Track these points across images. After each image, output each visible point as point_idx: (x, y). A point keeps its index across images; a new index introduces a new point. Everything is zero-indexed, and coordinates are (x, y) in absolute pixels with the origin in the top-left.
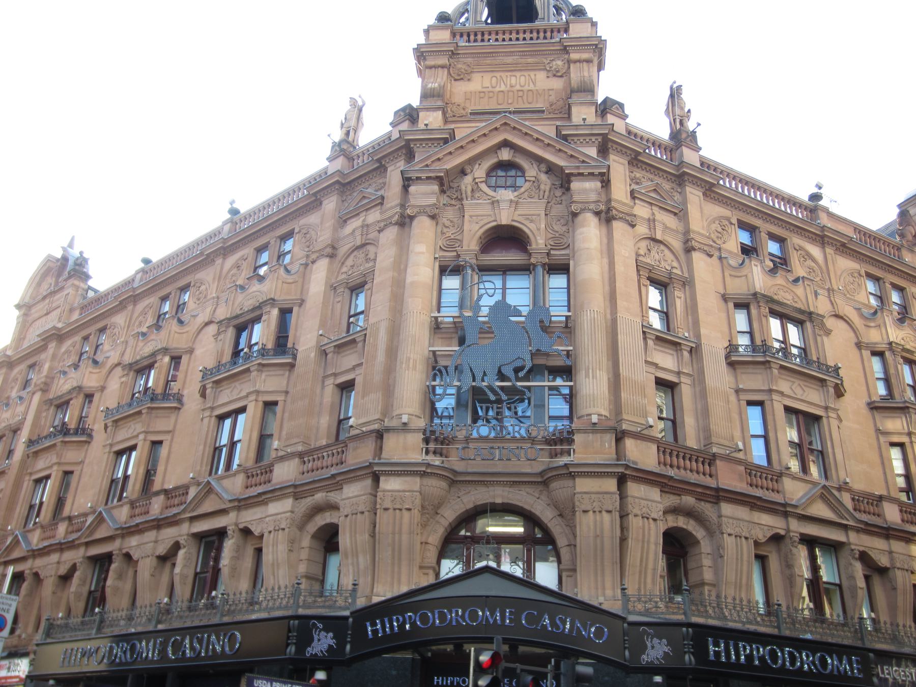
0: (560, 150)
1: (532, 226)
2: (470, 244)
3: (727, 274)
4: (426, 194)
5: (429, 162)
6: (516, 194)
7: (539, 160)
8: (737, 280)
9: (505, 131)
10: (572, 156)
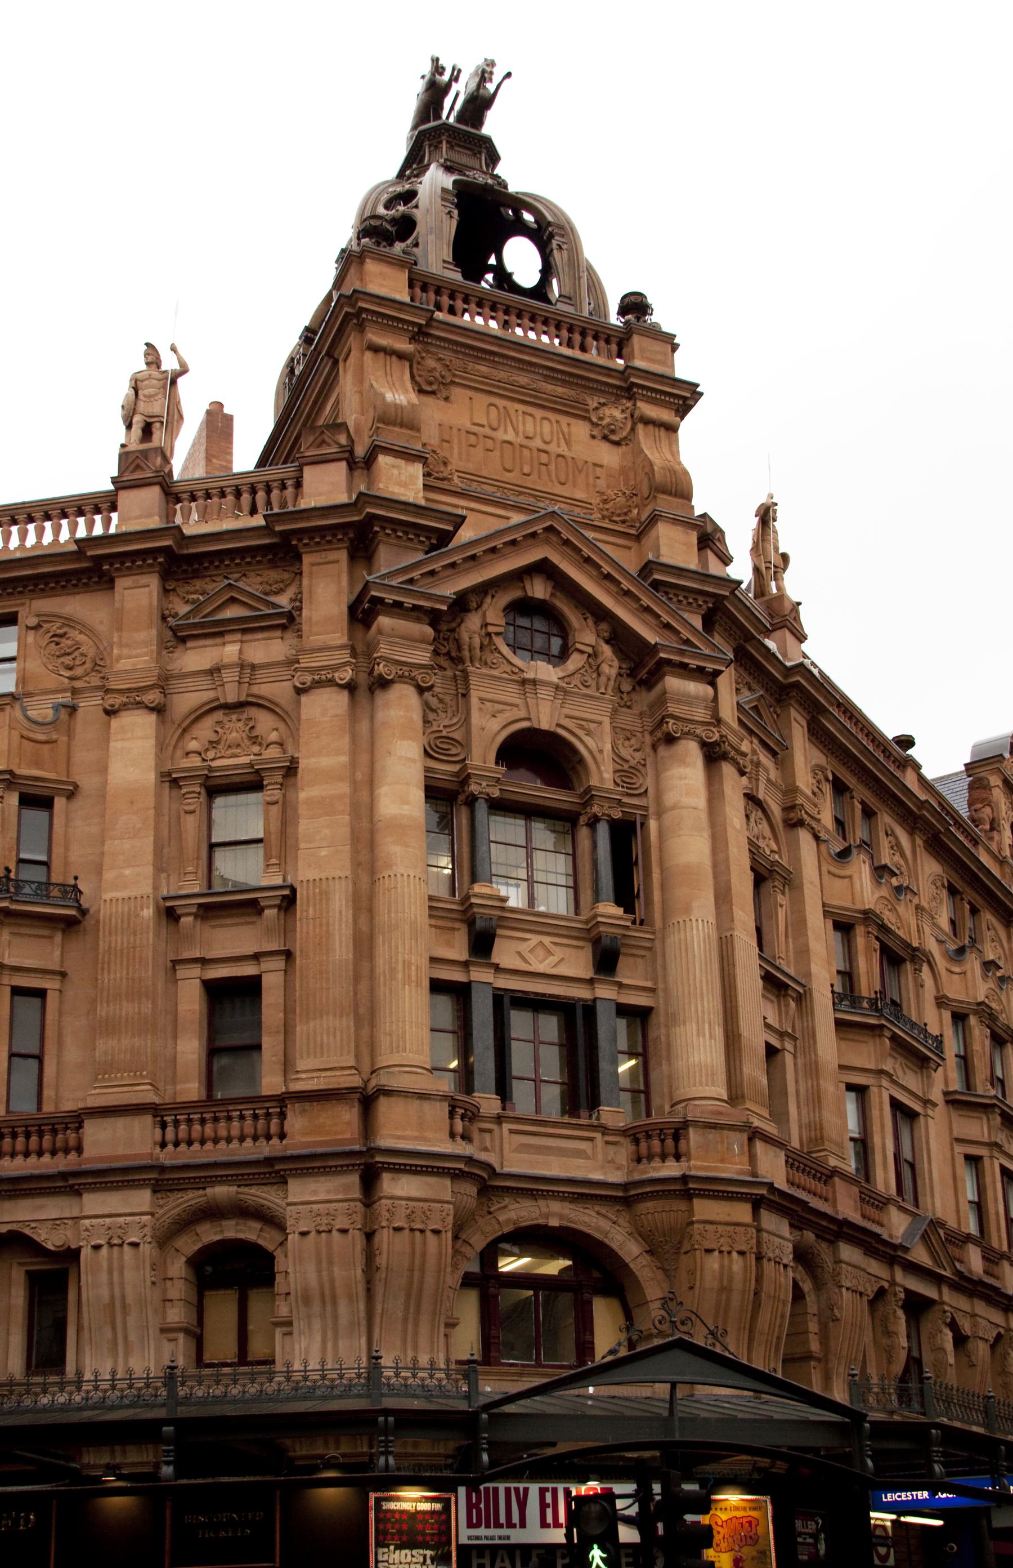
0: (648, 609)
2: (482, 757)
3: (824, 869)
4: (411, 640)
5: (415, 574)
7: (599, 613)
8: (838, 882)
9: (547, 542)
10: (667, 626)
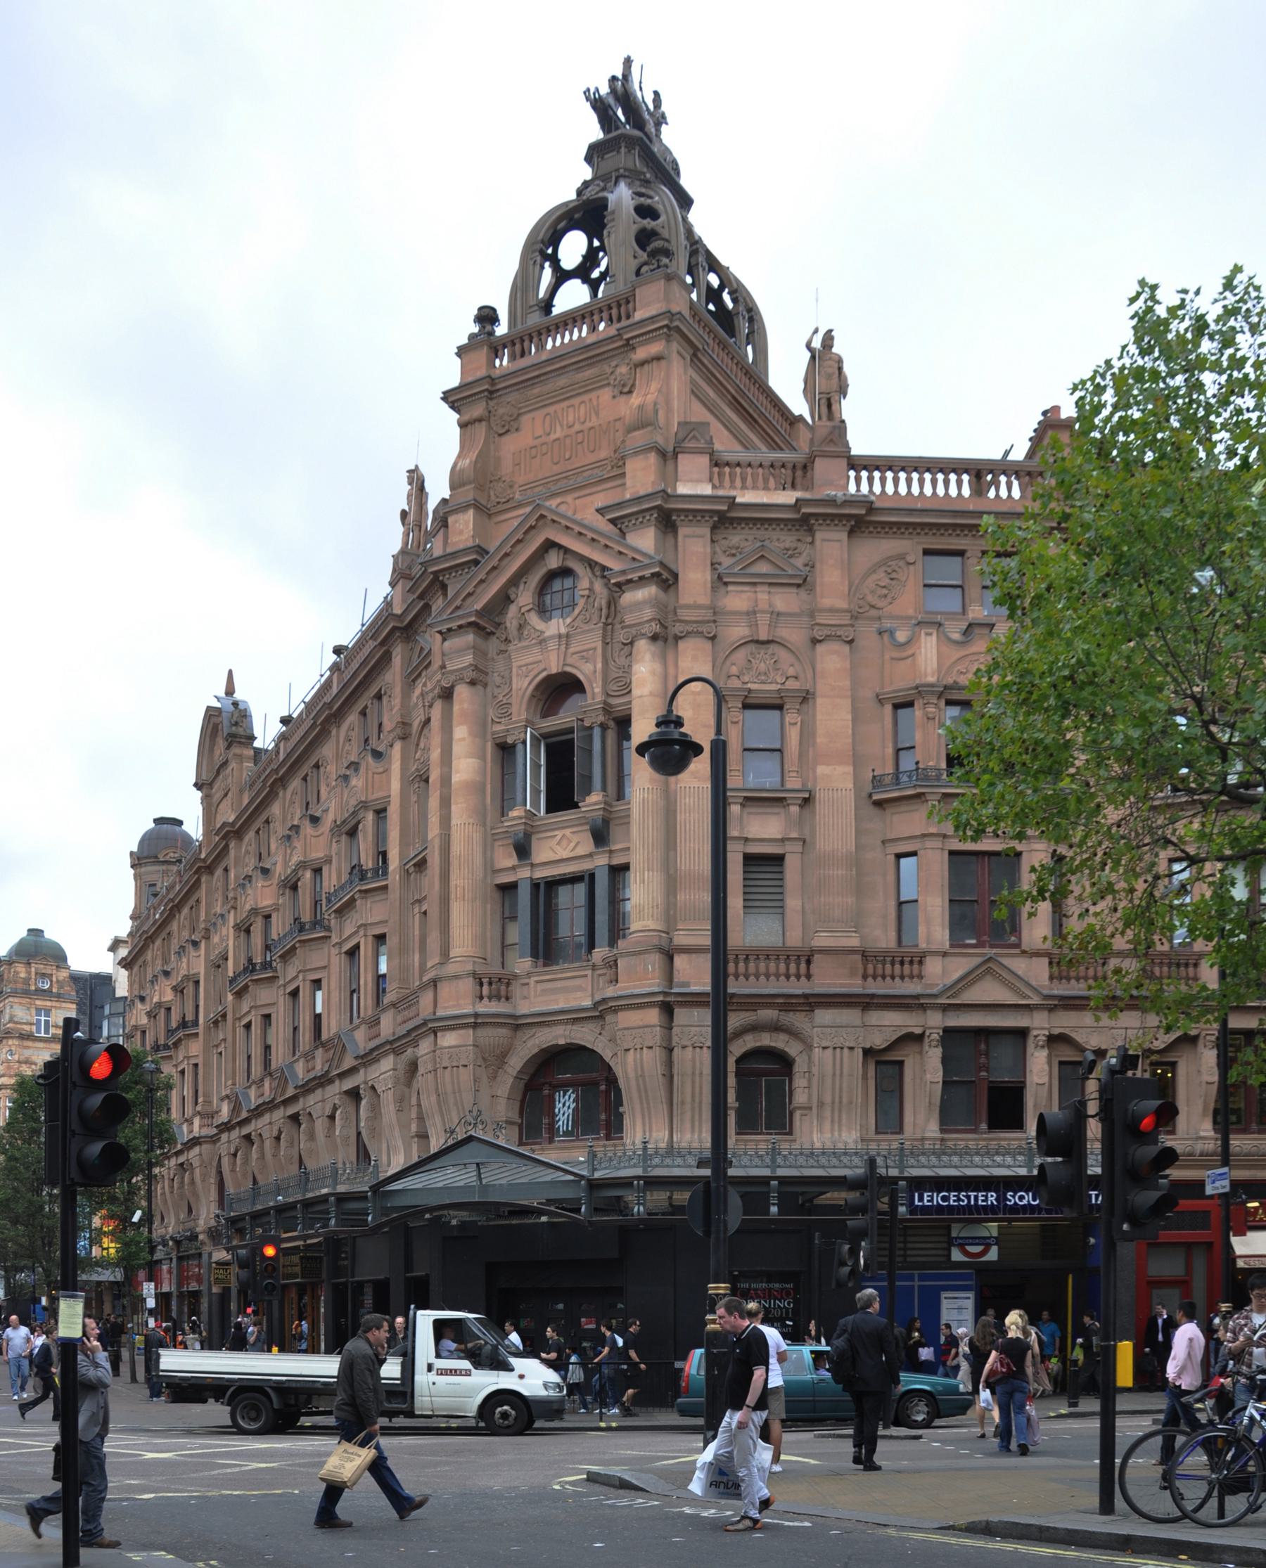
1: (587, 668)
6: (568, 620)
7: (591, 564)
